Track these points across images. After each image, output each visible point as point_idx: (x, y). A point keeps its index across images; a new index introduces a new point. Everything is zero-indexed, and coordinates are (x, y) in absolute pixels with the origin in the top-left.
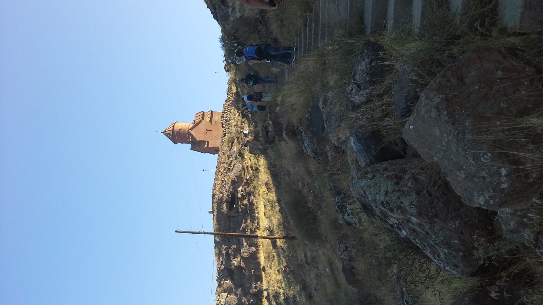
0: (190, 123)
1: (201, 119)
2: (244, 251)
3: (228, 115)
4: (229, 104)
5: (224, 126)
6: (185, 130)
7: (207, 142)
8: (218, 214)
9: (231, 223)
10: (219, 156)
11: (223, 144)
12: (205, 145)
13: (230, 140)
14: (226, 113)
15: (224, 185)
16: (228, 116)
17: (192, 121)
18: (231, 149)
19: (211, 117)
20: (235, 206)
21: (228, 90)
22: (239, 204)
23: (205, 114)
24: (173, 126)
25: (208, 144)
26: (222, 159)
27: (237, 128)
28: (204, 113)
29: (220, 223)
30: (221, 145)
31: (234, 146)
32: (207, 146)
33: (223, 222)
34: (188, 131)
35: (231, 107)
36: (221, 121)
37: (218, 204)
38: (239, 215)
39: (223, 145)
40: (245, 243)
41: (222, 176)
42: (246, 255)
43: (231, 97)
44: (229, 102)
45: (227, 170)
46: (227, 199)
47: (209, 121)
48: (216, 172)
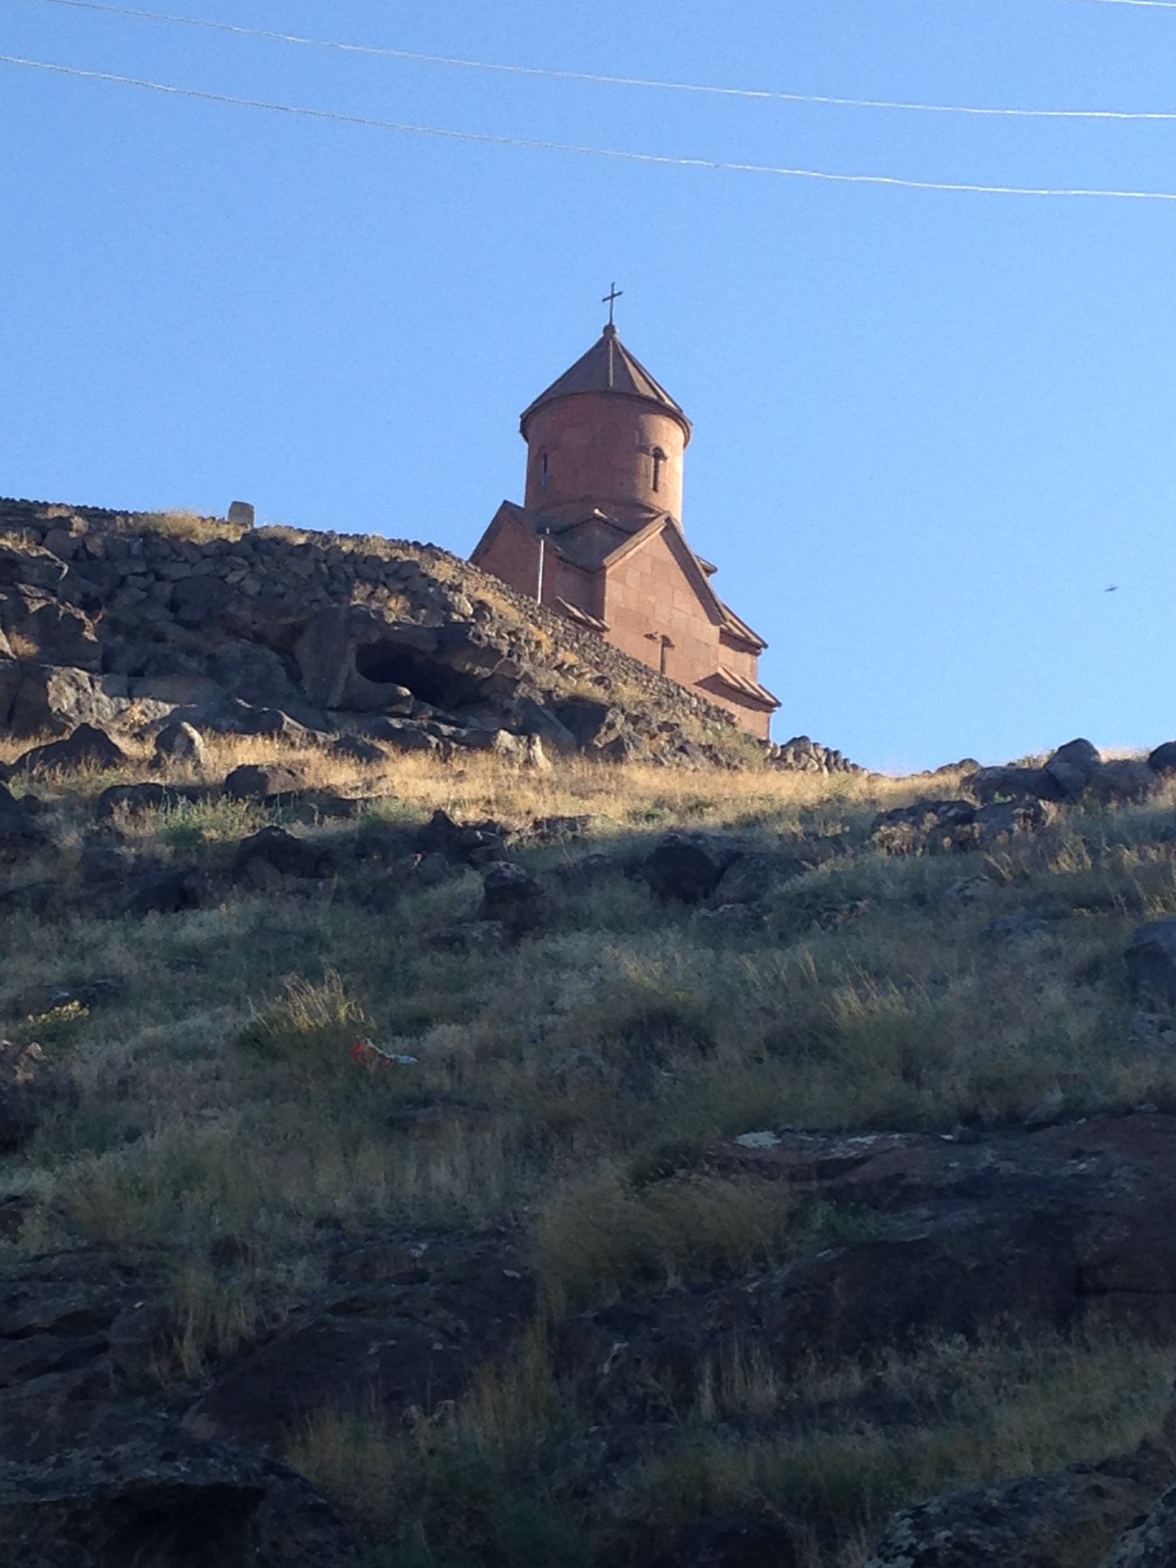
2: (90, 690)
6: (655, 489)
8: (312, 555)
9: (244, 640)
11: (696, 714)
15: (528, 642)
19: (738, 694)
20: (406, 691)
22: (446, 729)
23: (746, 658)
24: (676, 416)
29: (240, 560)
30: (695, 703)
33: (252, 587)
34: (651, 511)
37: (396, 572)
38: (331, 715)
40: (143, 713)
42: (65, 702)
46: (479, 638)
47: (718, 675)
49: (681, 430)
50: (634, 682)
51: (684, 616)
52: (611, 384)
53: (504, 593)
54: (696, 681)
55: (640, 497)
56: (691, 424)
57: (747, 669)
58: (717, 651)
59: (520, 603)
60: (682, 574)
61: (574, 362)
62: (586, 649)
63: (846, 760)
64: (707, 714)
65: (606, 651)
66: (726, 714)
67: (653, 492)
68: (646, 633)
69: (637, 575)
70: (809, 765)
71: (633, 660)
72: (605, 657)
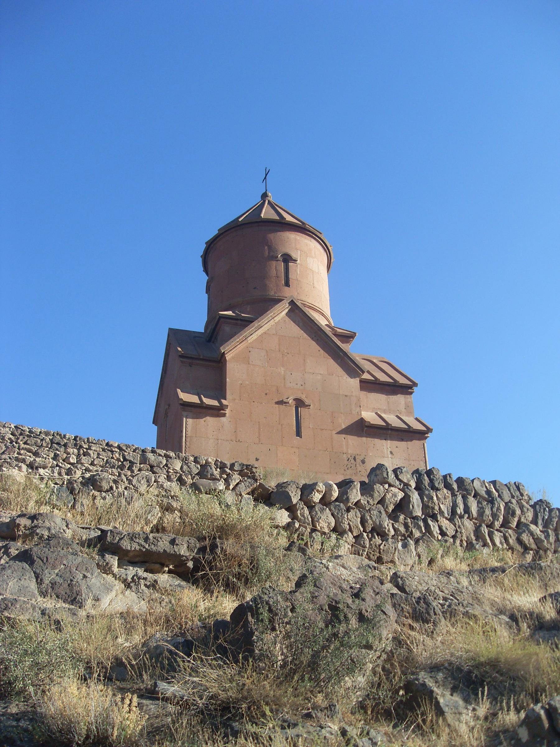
0: (328, 312)
1: (366, 376)
3: (451, 520)
4: (533, 527)
5: (355, 495)
6: (287, 284)
7: (215, 403)
11: (181, 481)
12: (199, 395)
14: (460, 510)
16: (445, 523)
17: (344, 327)
18: (115, 550)
23: (400, 399)
24: (302, 229)
30: (177, 465)
31: (153, 585)
35: (511, 548)
36: (395, 471)
39: (174, 487)
44: (546, 524)
47: (362, 419)
49: (313, 240)
50: (50, 462)
51: (319, 377)
52: (240, 220)
55: (272, 293)
56: (321, 233)
57: (402, 407)
60: (314, 343)
63: (445, 477)
64: (203, 472)
66: (237, 467)
68: (277, 400)
70: (389, 496)
71: (47, 434)
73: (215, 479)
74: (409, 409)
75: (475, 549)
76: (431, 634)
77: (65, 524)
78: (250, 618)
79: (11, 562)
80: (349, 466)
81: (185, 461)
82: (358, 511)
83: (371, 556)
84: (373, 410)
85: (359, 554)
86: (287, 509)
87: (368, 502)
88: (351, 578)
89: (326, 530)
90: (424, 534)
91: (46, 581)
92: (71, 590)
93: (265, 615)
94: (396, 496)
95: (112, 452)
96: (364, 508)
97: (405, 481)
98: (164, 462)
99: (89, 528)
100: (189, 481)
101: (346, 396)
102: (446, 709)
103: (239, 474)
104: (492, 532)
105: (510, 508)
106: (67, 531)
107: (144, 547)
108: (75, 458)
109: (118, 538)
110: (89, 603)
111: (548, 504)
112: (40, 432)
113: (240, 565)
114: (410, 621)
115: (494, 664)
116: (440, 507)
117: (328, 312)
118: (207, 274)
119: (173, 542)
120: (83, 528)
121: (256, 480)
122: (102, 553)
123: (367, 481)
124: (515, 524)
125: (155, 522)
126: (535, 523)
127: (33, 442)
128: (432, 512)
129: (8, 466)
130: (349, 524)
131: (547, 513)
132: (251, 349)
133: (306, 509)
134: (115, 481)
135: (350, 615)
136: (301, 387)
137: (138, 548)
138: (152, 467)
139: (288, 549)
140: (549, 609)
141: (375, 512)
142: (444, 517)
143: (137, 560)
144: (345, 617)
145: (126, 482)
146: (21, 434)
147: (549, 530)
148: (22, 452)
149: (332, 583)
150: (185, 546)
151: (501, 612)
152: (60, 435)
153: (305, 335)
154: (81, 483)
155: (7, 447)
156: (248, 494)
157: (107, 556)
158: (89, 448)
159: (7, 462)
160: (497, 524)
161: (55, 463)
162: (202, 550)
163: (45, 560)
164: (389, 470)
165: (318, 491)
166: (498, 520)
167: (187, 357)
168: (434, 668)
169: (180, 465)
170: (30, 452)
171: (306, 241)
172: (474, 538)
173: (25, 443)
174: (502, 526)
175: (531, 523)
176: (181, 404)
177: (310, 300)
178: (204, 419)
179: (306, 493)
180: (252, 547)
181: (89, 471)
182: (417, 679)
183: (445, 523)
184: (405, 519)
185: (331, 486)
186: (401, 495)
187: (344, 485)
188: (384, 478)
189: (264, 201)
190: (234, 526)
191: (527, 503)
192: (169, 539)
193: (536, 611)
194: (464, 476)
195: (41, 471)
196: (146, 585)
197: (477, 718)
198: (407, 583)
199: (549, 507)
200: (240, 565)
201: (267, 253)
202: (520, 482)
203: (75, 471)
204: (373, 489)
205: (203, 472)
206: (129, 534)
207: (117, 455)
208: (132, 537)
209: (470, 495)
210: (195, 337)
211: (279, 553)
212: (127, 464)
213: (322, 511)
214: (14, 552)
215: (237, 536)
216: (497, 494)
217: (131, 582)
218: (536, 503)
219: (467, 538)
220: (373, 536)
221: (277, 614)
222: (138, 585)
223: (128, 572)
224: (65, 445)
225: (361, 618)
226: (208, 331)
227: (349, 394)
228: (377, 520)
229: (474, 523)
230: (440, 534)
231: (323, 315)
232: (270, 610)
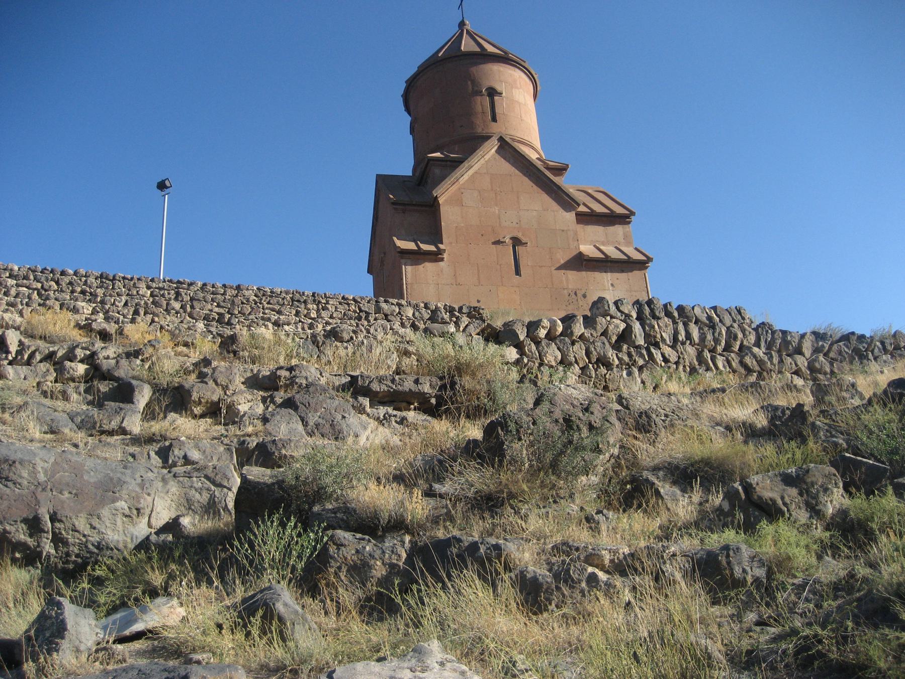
1: (582, 209)
3: (673, 347)
4: (756, 350)
5: (579, 328)
6: (494, 119)
7: (432, 248)
10: (297, 300)
11: (414, 327)
12: (415, 241)
13: (467, 382)
14: (682, 336)
16: (667, 351)
17: (556, 159)
18: (366, 392)
19: (605, 264)
21: (846, 338)
23: (618, 230)
24: (504, 59)
25: (418, 257)
26: (266, 332)
27: (613, 419)
28: (623, 219)
30: (409, 312)
31: (402, 421)
32: (405, 253)
35: (734, 371)
36: (616, 303)
39: (408, 332)
41: (77, 336)
43: (802, 362)
44: (769, 347)
45: (121, 373)
47: (580, 253)
48: (130, 283)
49: (517, 70)
50: (293, 319)
51: (535, 213)
53: (26, 278)
54: (558, 265)
55: (479, 130)
57: (620, 238)
58: (576, 233)
59: (57, 283)
60: (526, 181)
61: (431, 54)
62: (195, 303)
63: (665, 306)
64: (434, 318)
65: (237, 296)
66: (465, 310)
67: (494, 123)
68: (493, 241)
69: (476, 194)
70: (611, 327)
71: (287, 293)
72: (233, 303)
73: (444, 322)
74: (627, 239)
75: (698, 373)
76: (653, 443)
77: (319, 373)
78: (500, 431)
79: (278, 410)
80: (570, 301)
81: (416, 307)
82: (583, 345)
83: (598, 385)
84: (591, 242)
85: (586, 384)
86: (515, 347)
87: (591, 334)
88: (580, 396)
89: (554, 364)
90: (647, 362)
91: (311, 423)
92: (334, 429)
93: (512, 426)
94: (618, 327)
95: (348, 304)
96: (588, 341)
97: (626, 312)
98: (397, 310)
99: (339, 375)
100: (422, 326)
101: (563, 231)
102: (666, 497)
103: (467, 316)
104: (715, 356)
105: (731, 332)
106: (322, 379)
107: (392, 388)
108: (315, 312)
109: (367, 382)
110: (350, 440)
111: (770, 327)
112: (281, 292)
113: (478, 398)
114: (634, 433)
115: (706, 462)
116: (662, 336)
117: (537, 144)
118: (409, 114)
119: (417, 382)
120: (336, 375)
121: (484, 321)
122: (355, 395)
123: (589, 315)
124: (738, 347)
125: (394, 367)
126: (757, 344)
127: (275, 301)
128: (655, 340)
129: (255, 325)
130: (575, 356)
131: (770, 335)
132: (463, 190)
133: (533, 345)
134: (354, 332)
135: (581, 426)
136: (517, 226)
137: (386, 389)
138: (386, 316)
139: (521, 381)
140: (761, 419)
141: (599, 344)
142: (666, 344)
143: (386, 400)
144: (577, 426)
145: (365, 332)
146: (264, 295)
147: (773, 352)
148: (267, 311)
149: (565, 401)
150: (428, 384)
151: (718, 424)
152: (299, 293)
153: (517, 171)
154: (324, 335)
155: (252, 308)
156: (478, 334)
157: (360, 398)
158: (327, 303)
159: (254, 322)
160: (719, 349)
161: (298, 319)
162: (443, 387)
163: (307, 405)
164: (610, 302)
165: (543, 327)
166: (720, 344)
167: (400, 204)
168: (655, 469)
169: (412, 312)
170: (273, 311)
171: (510, 72)
172: (696, 363)
173: (269, 303)
174: (724, 350)
175: (754, 345)
176: (399, 252)
177: (519, 134)
178: (423, 265)
179: (532, 330)
180: (488, 382)
181: (329, 324)
182: (641, 476)
183: (667, 351)
184: (628, 348)
185: (555, 321)
186: (623, 326)
187: (568, 320)
188: (606, 310)
189: (462, 31)
190: (468, 365)
191: (750, 326)
192: (413, 379)
193: (749, 421)
194: (684, 304)
195: (286, 327)
196: (396, 422)
197: (691, 503)
198: (631, 403)
199: (771, 330)
200: (478, 398)
201: (470, 88)
202: (741, 305)
203: (317, 326)
204: (595, 323)
205: (434, 318)
206: (377, 377)
207: (353, 307)
208: (380, 380)
209: (691, 321)
210: (405, 181)
211: (514, 385)
212: (363, 315)
213: (548, 345)
214: (279, 400)
215: (473, 375)
216: (718, 319)
217: (383, 420)
218: (758, 326)
219: (690, 363)
220: (598, 367)
221: (521, 427)
222: (389, 422)
223: (380, 411)
224: (305, 302)
225: (591, 427)
226: (417, 174)
227: (565, 229)
228: (602, 352)
229: (696, 348)
230: (663, 361)
231: (533, 148)
232: (516, 423)
